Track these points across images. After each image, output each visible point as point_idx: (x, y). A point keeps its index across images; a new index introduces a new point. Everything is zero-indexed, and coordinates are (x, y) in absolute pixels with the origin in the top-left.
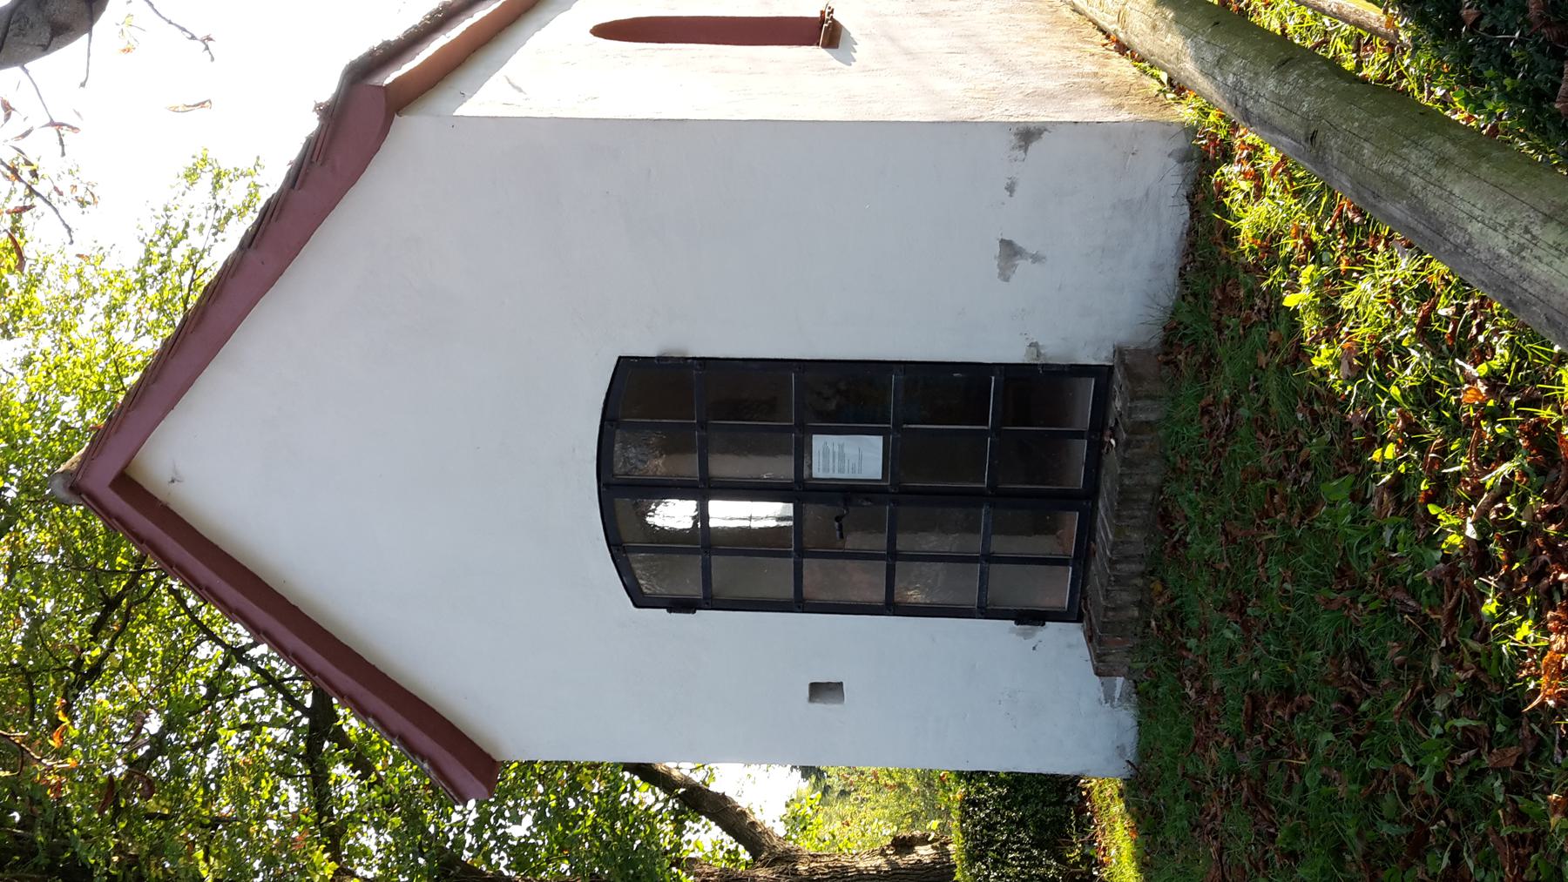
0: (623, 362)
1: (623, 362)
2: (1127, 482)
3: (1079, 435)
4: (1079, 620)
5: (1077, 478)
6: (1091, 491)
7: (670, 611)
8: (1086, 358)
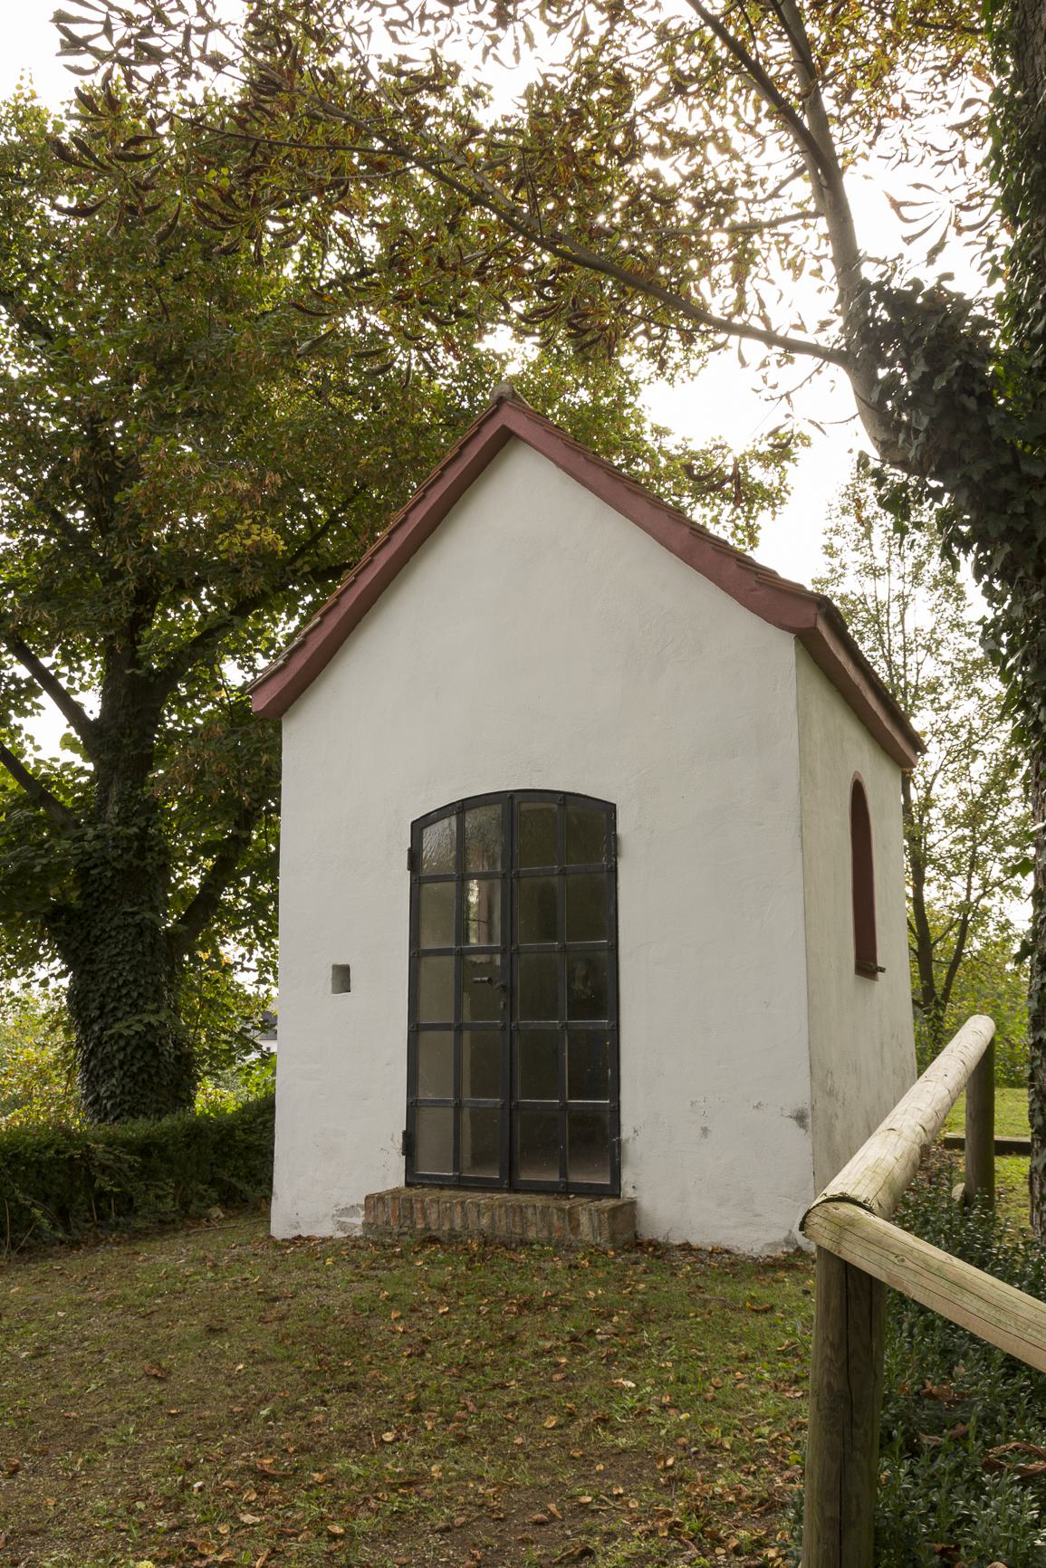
0: (610, 809)
1: (610, 809)
2: (530, 1211)
3: (563, 1174)
4: (408, 1184)
5: (526, 1176)
6: (514, 1188)
7: (410, 850)
8: (627, 1176)
